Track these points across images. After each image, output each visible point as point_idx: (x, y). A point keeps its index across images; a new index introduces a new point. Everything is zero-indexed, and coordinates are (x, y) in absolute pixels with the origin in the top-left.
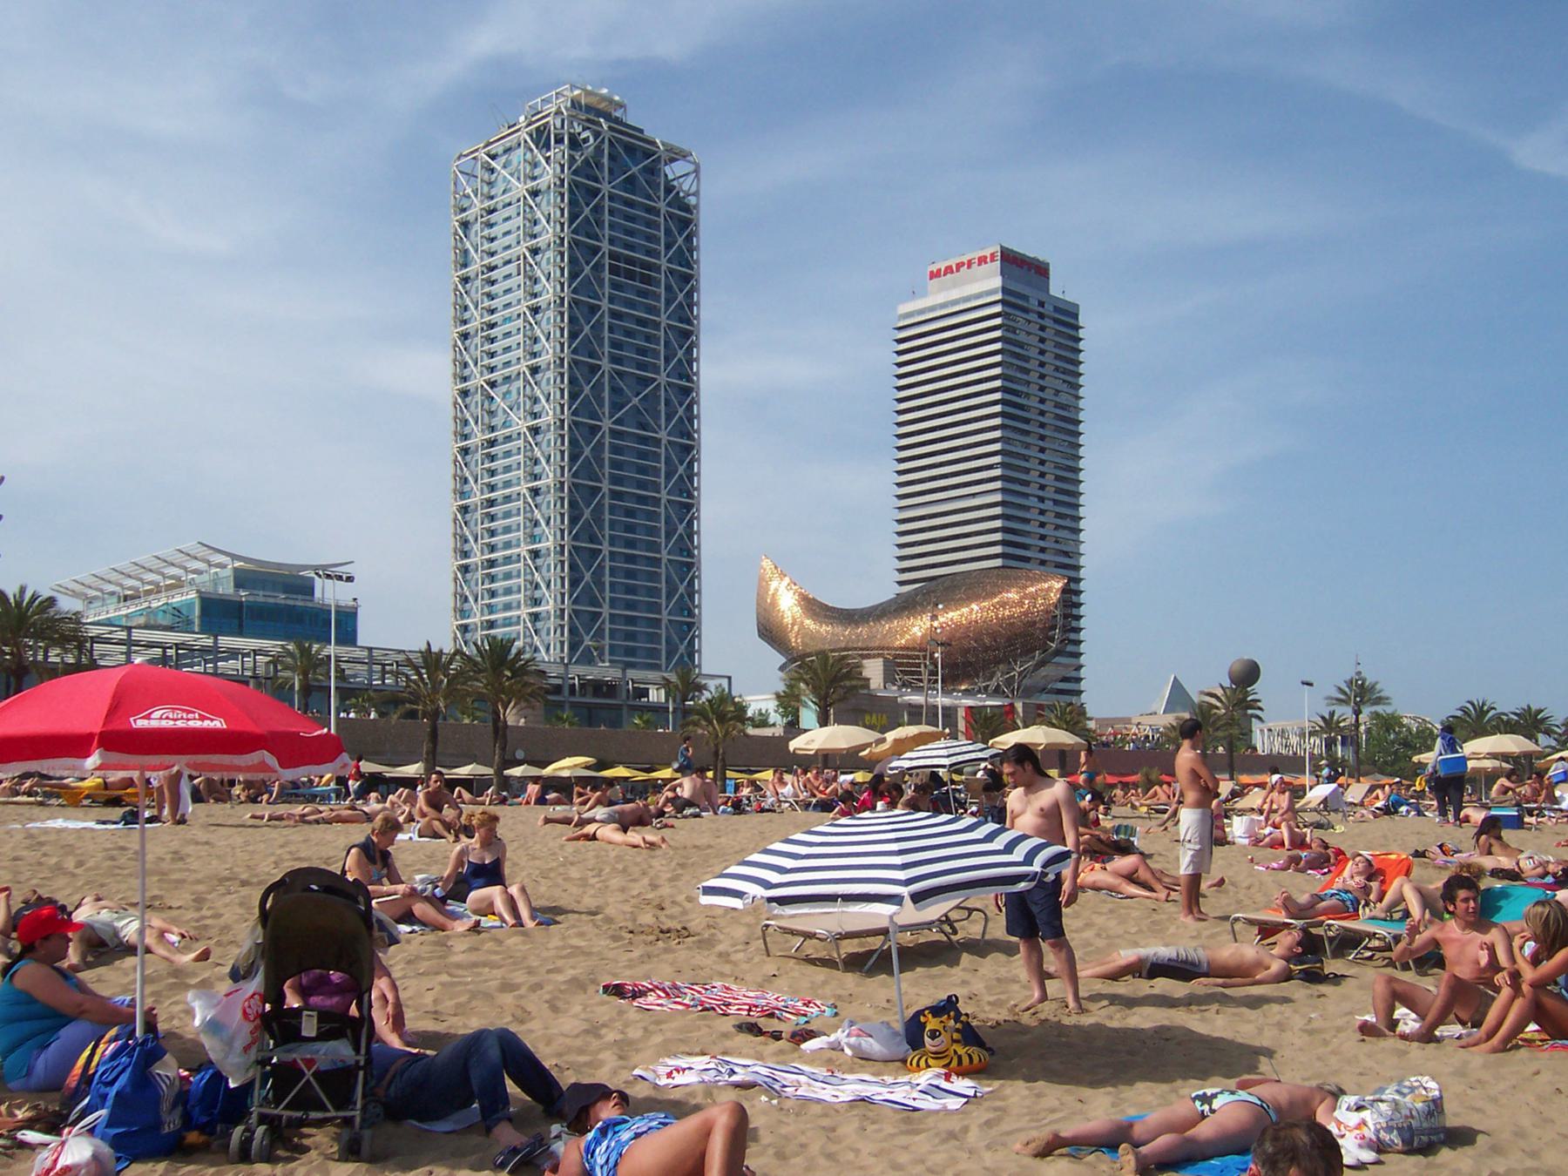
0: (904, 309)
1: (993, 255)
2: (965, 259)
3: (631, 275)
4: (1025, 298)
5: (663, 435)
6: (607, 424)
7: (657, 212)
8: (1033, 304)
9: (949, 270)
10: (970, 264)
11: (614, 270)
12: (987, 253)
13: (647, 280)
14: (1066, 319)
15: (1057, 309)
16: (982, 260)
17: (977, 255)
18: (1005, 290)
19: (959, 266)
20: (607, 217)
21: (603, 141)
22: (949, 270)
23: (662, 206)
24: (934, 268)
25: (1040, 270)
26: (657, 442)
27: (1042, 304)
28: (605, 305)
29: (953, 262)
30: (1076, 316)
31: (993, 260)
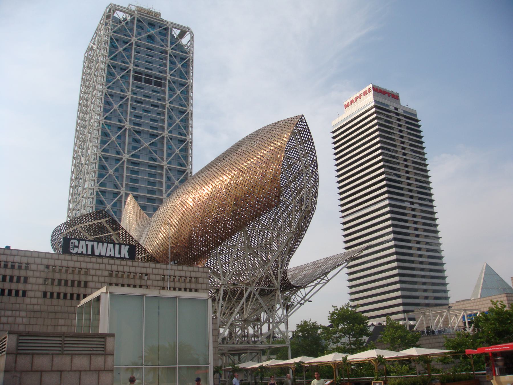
0: (334, 123)
1: (369, 89)
2: (358, 95)
3: (148, 82)
4: (388, 106)
5: (165, 164)
6: (126, 157)
7: (166, 52)
8: (392, 108)
9: (352, 102)
10: (360, 96)
11: (136, 78)
12: (366, 89)
13: (159, 84)
14: (411, 121)
15: (404, 111)
16: (365, 93)
17: (362, 91)
18: (375, 101)
19: (356, 98)
20: (133, 53)
21: (134, 18)
22: (352, 102)
23: (169, 49)
24: (346, 103)
25: (396, 97)
26: (161, 167)
27: (396, 109)
28: (129, 95)
29: (353, 98)
30: (416, 115)
31: (370, 91)
